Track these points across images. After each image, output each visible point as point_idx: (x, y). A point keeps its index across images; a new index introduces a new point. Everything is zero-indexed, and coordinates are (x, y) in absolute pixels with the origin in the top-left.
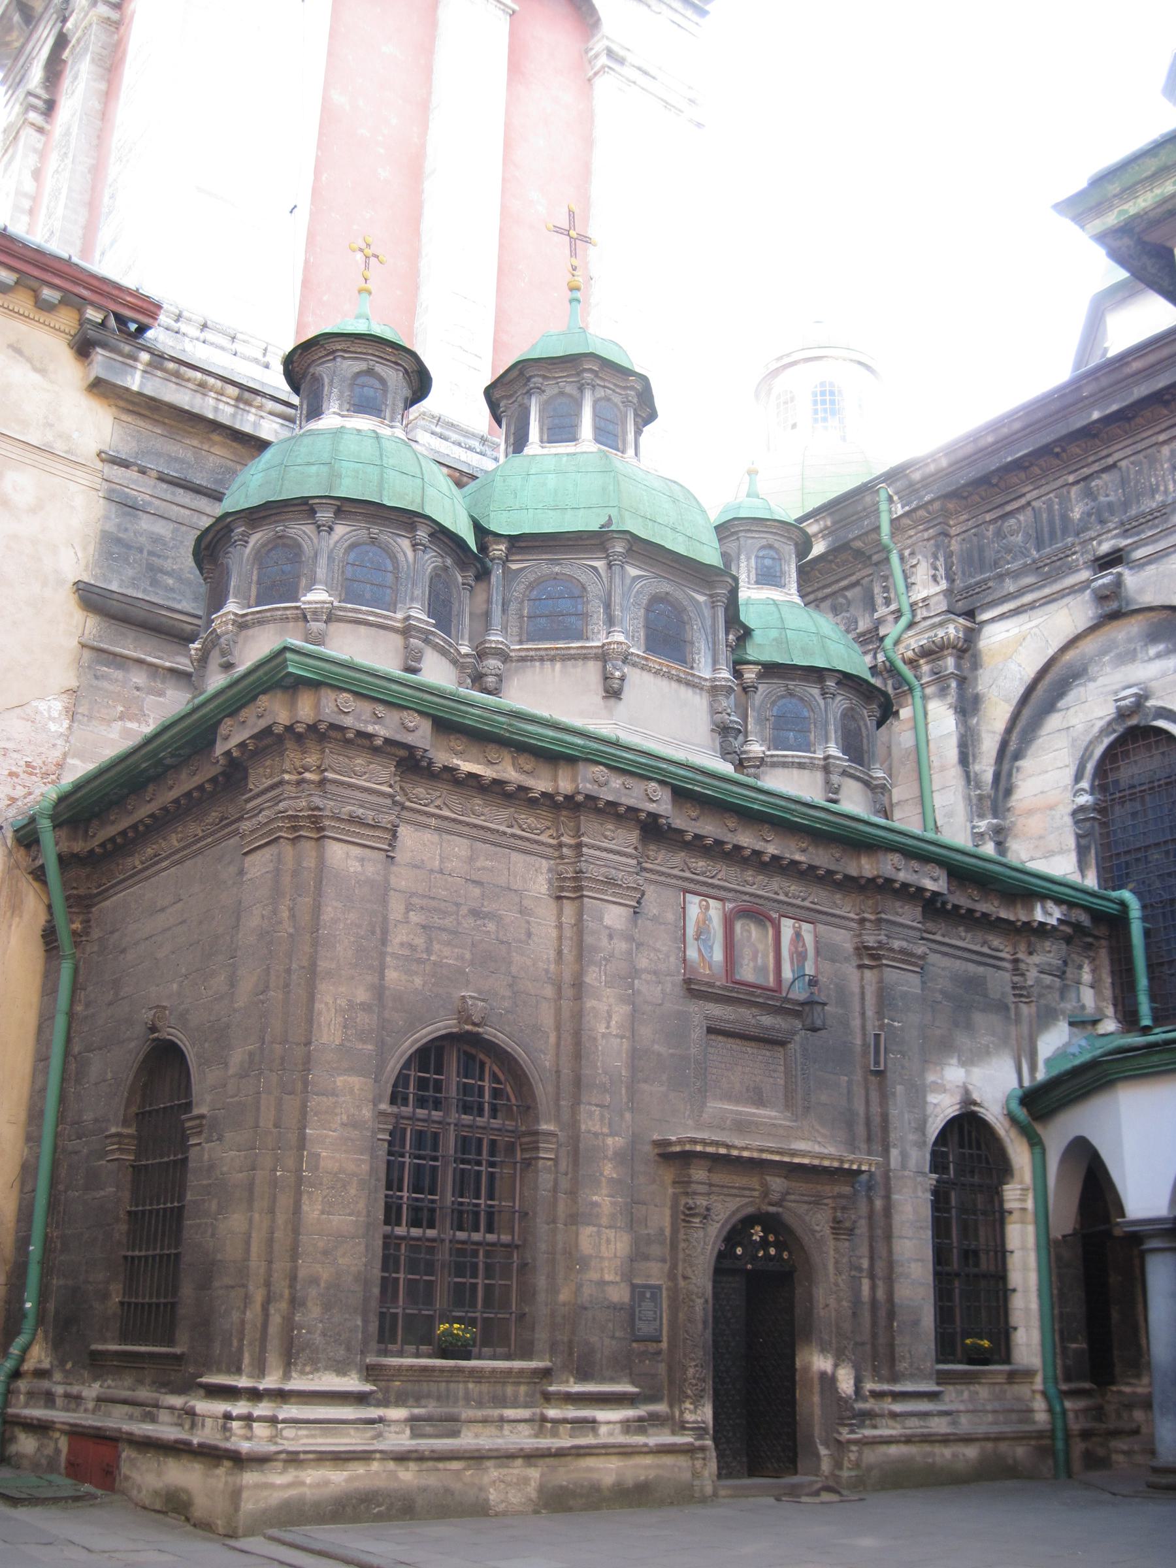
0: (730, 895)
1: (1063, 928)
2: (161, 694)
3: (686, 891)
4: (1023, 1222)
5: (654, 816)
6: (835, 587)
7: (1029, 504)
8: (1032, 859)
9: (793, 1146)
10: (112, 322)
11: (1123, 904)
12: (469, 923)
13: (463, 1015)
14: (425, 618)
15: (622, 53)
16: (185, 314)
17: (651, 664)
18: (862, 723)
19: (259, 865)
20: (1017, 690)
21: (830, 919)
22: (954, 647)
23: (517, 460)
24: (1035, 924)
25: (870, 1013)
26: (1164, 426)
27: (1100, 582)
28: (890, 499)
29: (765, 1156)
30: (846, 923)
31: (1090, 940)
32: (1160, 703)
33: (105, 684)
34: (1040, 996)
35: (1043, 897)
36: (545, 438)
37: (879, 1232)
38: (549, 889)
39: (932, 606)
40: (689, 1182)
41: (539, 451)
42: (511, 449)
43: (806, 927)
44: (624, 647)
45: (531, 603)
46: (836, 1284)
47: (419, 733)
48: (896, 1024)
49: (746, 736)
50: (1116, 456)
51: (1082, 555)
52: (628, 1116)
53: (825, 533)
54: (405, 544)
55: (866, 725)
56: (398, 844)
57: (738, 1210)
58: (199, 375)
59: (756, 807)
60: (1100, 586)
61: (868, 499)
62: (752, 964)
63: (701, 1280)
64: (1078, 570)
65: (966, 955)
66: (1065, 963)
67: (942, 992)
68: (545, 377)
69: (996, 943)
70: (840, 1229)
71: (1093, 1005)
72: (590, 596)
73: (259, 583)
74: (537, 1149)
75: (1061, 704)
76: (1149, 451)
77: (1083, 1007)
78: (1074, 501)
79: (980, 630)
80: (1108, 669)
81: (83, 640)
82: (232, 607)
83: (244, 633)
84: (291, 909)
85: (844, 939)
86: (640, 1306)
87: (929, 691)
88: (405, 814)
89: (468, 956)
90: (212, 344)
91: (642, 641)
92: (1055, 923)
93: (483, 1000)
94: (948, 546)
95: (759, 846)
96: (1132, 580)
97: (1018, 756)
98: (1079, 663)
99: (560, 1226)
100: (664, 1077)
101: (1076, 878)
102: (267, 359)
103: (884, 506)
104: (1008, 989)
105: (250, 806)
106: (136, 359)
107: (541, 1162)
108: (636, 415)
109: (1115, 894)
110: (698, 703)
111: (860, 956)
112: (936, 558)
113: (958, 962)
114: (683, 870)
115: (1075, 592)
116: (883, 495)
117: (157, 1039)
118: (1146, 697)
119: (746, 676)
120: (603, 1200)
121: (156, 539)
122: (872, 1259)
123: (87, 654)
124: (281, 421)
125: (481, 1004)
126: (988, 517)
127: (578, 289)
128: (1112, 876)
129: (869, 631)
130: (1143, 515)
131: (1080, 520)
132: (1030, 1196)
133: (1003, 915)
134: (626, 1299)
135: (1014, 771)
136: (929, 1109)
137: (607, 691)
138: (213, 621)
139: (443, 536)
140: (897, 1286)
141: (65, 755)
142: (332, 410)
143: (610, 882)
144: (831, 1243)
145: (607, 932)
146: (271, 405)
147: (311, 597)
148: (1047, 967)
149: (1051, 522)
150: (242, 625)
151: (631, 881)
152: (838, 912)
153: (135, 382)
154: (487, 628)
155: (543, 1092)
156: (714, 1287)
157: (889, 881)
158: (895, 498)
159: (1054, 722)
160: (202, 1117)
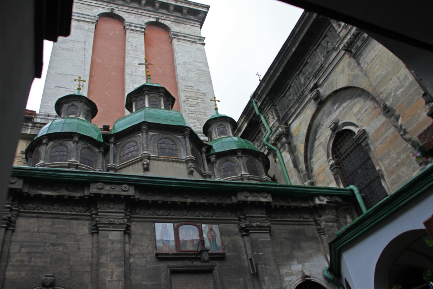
0: (176, 220)
5: (128, 197)
6: (255, 135)
11: (352, 191)
12: (51, 248)
15: (177, 34)
16: (50, 114)
17: (160, 158)
18: (256, 164)
22: (284, 134)
26: (314, 43)
27: (313, 95)
31: (345, 207)
32: (342, 122)
34: (328, 230)
35: (318, 195)
38: (89, 231)
44: (147, 154)
45: (123, 152)
47: (17, 183)
48: (260, 253)
50: (306, 60)
51: (307, 91)
53: (245, 120)
55: (257, 164)
59: (173, 185)
60: (313, 96)
61: (251, 106)
62: (191, 244)
64: (308, 96)
67: (284, 238)
68: (136, 97)
72: (138, 144)
75: (317, 137)
76: (314, 53)
78: (301, 78)
80: (326, 120)
85: (234, 228)
87: (281, 150)
89: (49, 260)
91: (157, 152)
92: (325, 203)
94: (275, 108)
95: (183, 200)
96: (321, 90)
97: (311, 158)
103: (254, 105)
104: (316, 231)
109: (348, 188)
110: (183, 167)
112: (272, 112)
113: (290, 227)
114: (152, 215)
115: (309, 103)
116: (254, 102)
118: (338, 122)
119: (212, 159)
125: (49, 278)
127: (149, 76)
130: (318, 70)
133: (303, 205)
135: (311, 163)
137: (144, 169)
145: (111, 241)
148: (329, 220)
149: (297, 87)
151: (121, 222)
152: (229, 218)
158: (257, 101)
159: (317, 143)
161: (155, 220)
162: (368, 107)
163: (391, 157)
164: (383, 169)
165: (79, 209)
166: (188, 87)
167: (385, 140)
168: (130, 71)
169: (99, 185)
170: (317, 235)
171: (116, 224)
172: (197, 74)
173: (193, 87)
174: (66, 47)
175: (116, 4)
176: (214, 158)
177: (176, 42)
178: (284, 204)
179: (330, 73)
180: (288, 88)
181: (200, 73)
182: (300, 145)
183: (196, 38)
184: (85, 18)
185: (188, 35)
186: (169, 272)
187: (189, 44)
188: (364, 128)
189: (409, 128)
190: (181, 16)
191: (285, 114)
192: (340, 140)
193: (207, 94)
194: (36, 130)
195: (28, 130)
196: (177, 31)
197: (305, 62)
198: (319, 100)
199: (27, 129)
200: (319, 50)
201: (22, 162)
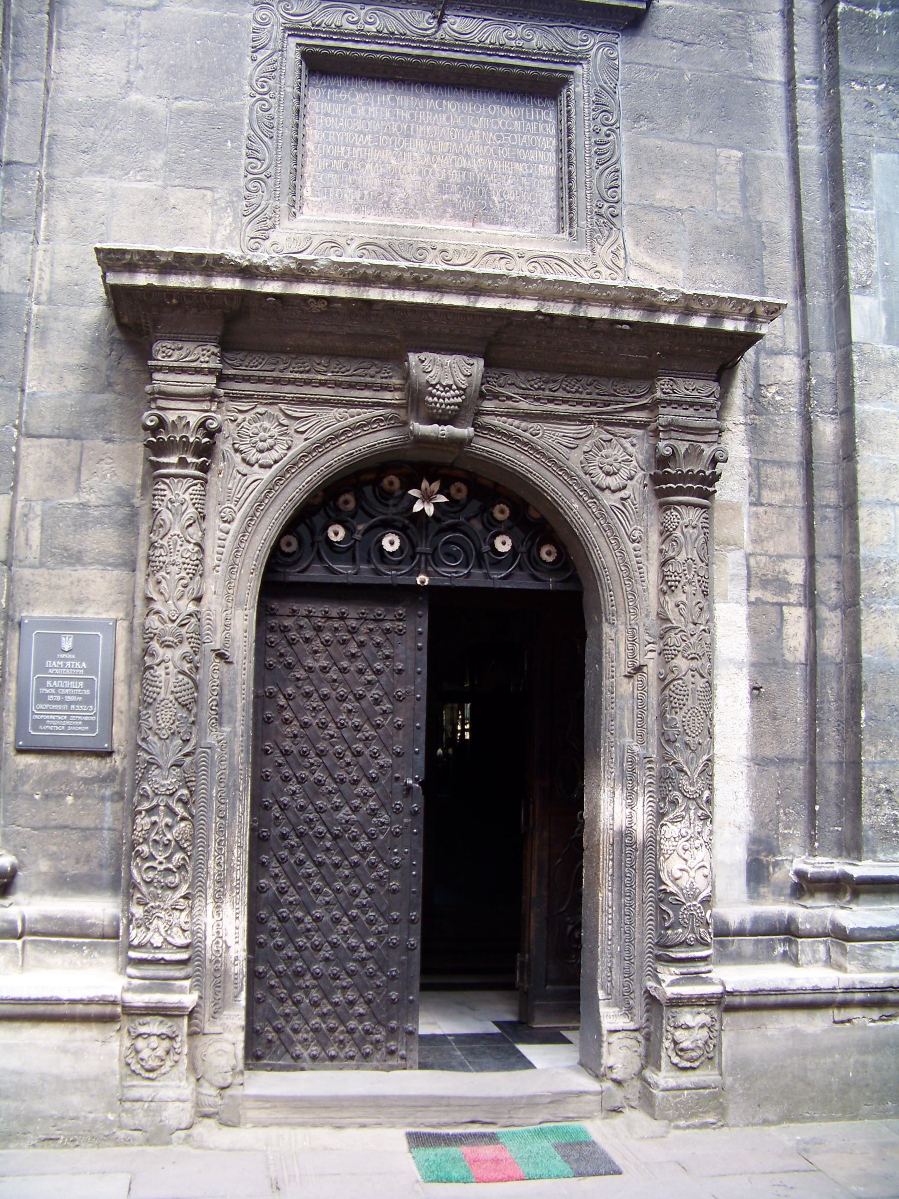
29: (374, 294)
37: (828, 496)
57: (334, 438)
86: (41, 667)
100: (158, 160)
122: (811, 560)
140: (869, 623)
186: (293, 54)
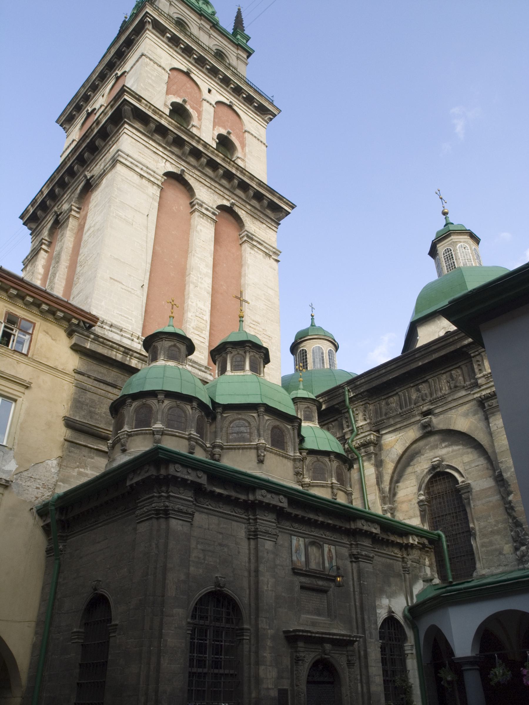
0: (306, 536)
1: (419, 545)
2: (92, 458)
3: (291, 535)
4: (412, 659)
5: (282, 508)
7: (397, 393)
8: (404, 519)
9: (331, 632)
10: (82, 324)
11: (439, 536)
13: (217, 584)
14: (195, 434)
15: (251, 236)
16: (105, 321)
17: (273, 451)
19: (143, 528)
20: (395, 458)
21: (340, 544)
22: (373, 443)
23: (223, 377)
24: (410, 544)
25: (355, 579)
27: (424, 420)
28: (349, 390)
29: (324, 636)
30: (346, 545)
32: (448, 463)
33: (72, 454)
35: (412, 534)
36: (233, 369)
37: (363, 664)
38: (245, 535)
39: (364, 428)
40: (298, 647)
41: (230, 374)
42: (220, 372)
43: (332, 547)
44: (265, 445)
45: (231, 428)
46: (350, 686)
49: (303, 476)
50: (427, 378)
52: (275, 621)
54: (189, 407)
56: (194, 519)
58: (111, 343)
61: (341, 391)
62: (314, 562)
63: (303, 687)
64: (415, 417)
65: (386, 556)
66: (420, 557)
68: (232, 348)
69: (396, 551)
70: (350, 664)
71: (430, 574)
72: (252, 426)
73: (136, 420)
74: (243, 635)
75: (412, 463)
76: (439, 376)
77: (427, 574)
79: (381, 437)
81: (66, 438)
82: (126, 428)
83: (130, 438)
84: (156, 544)
85: (345, 552)
87: (364, 458)
88: (197, 508)
89: (218, 561)
90: (114, 332)
91: (270, 442)
92: (416, 543)
93: (224, 578)
95: (316, 518)
97: (398, 481)
98: (417, 449)
99: (252, 666)
101: (421, 526)
102: (132, 338)
105: (139, 505)
106: (89, 337)
107: (244, 641)
108: (264, 361)
109: (436, 532)
110: (290, 464)
111: (351, 558)
113: (384, 559)
114: (290, 527)
115: (415, 424)
116: (347, 389)
117: (97, 593)
118: (442, 461)
120: (267, 655)
121: (93, 401)
122: (361, 675)
123: (66, 443)
124: (138, 360)
125: (223, 579)
126: (383, 398)
128: (434, 525)
129: (341, 437)
131: (415, 399)
132: (414, 647)
133: (399, 540)
134: (277, 695)
135: (396, 487)
136: (378, 615)
137: (258, 461)
138: (119, 433)
139: (201, 405)
141: (57, 481)
142: (161, 359)
143: (267, 533)
144: (347, 669)
146: (135, 354)
147: (156, 426)
148: (414, 560)
150: (130, 435)
151: (274, 532)
153: (88, 345)
154: (216, 437)
155: (245, 613)
156: (307, 689)
157: (361, 530)
158: (350, 390)
159: (410, 470)
160: (116, 625)
161: (291, 532)
162: (480, 463)
163: (489, 521)
164: (477, 528)
165: (238, 510)
166: (254, 323)
167: (487, 503)
168: (196, 280)
169: (264, 492)
170: (402, 572)
171: (271, 534)
172: (266, 305)
173: (259, 324)
174: (125, 216)
175: (188, 163)
176: (305, 454)
177: (249, 249)
178: (385, 537)
179: (451, 409)
180: (392, 394)
181: (269, 305)
182: (389, 463)
183: (271, 249)
184: (150, 174)
185: (264, 241)
187: (263, 256)
188: (469, 482)
189: (517, 508)
190: (259, 209)
191: (380, 421)
192: (438, 479)
193: (273, 338)
194: (96, 345)
195: (88, 344)
196: (251, 231)
197: (425, 379)
198: (429, 429)
199: (86, 340)
200: (446, 376)
201: (74, 385)
